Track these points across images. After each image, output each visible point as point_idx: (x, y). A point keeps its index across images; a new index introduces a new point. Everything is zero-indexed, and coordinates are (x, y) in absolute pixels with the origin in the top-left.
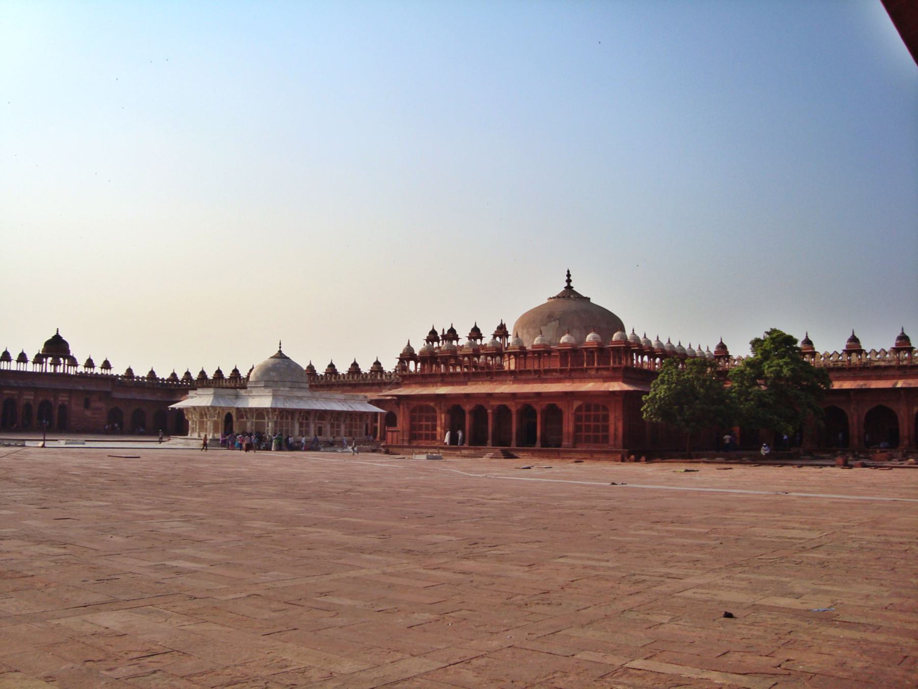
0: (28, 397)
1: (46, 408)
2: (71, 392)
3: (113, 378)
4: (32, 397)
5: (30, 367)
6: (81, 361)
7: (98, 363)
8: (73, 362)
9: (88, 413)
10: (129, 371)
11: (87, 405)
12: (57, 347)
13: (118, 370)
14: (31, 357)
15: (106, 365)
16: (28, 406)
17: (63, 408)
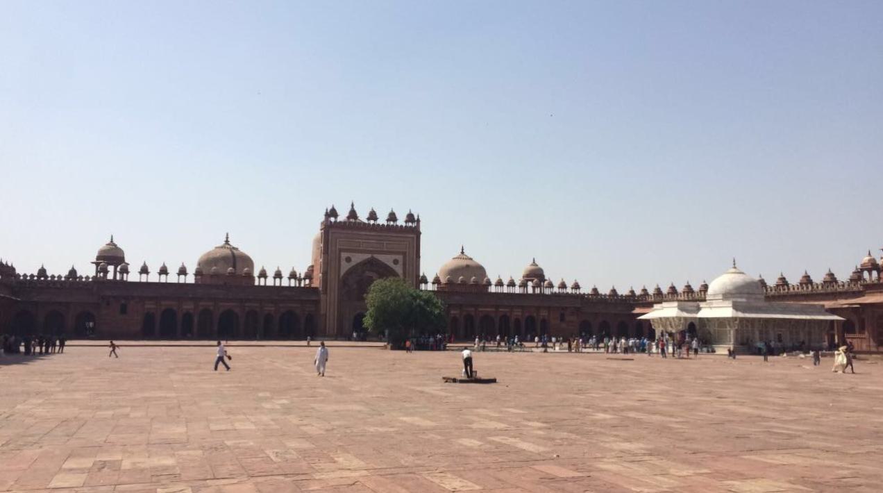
0: (517, 313)
1: (531, 322)
2: (549, 308)
3: (582, 296)
4: (520, 314)
5: (517, 290)
6: (556, 283)
7: (569, 284)
8: (551, 285)
9: (564, 325)
10: (595, 290)
11: (562, 319)
12: (536, 275)
13: (586, 289)
14: (518, 282)
15: (577, 286)
16: (517, 321)
17: (544, 321)
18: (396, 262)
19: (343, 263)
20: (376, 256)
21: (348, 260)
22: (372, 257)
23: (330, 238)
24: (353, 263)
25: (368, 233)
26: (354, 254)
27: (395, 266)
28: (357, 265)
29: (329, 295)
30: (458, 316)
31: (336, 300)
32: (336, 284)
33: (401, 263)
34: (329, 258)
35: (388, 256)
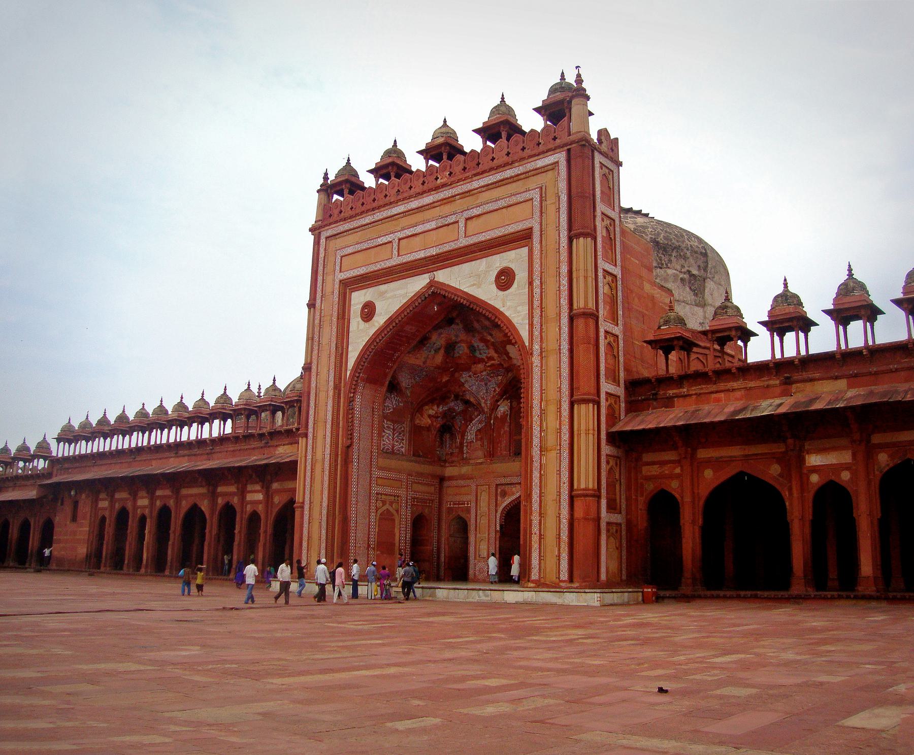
18: (505, 279)
19: (356, 322)
20: (444, 276)
21: (368, 312)
22: (432, 283)
23: (322, 255)
24: (380, 320)
25: (414, 204)
26: (383, 288)
27: (501, 293)
28: (390, 321)
29: (310, 442)
30: (846, 476)
31: (328, 451)
32: (330, 408)
33: (521, 276)
34: (317, 317)
35: (481, 265)
